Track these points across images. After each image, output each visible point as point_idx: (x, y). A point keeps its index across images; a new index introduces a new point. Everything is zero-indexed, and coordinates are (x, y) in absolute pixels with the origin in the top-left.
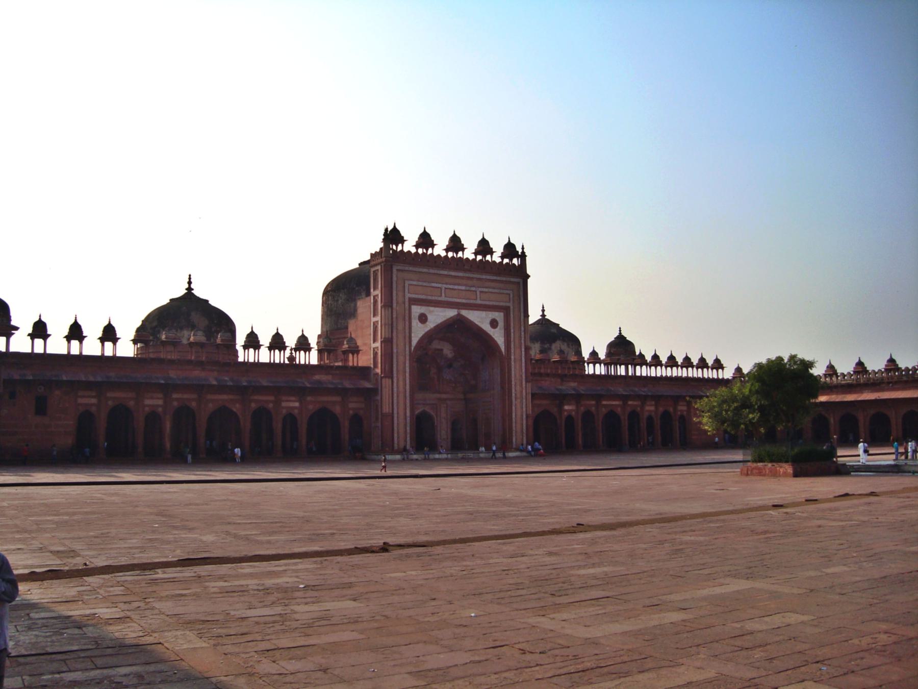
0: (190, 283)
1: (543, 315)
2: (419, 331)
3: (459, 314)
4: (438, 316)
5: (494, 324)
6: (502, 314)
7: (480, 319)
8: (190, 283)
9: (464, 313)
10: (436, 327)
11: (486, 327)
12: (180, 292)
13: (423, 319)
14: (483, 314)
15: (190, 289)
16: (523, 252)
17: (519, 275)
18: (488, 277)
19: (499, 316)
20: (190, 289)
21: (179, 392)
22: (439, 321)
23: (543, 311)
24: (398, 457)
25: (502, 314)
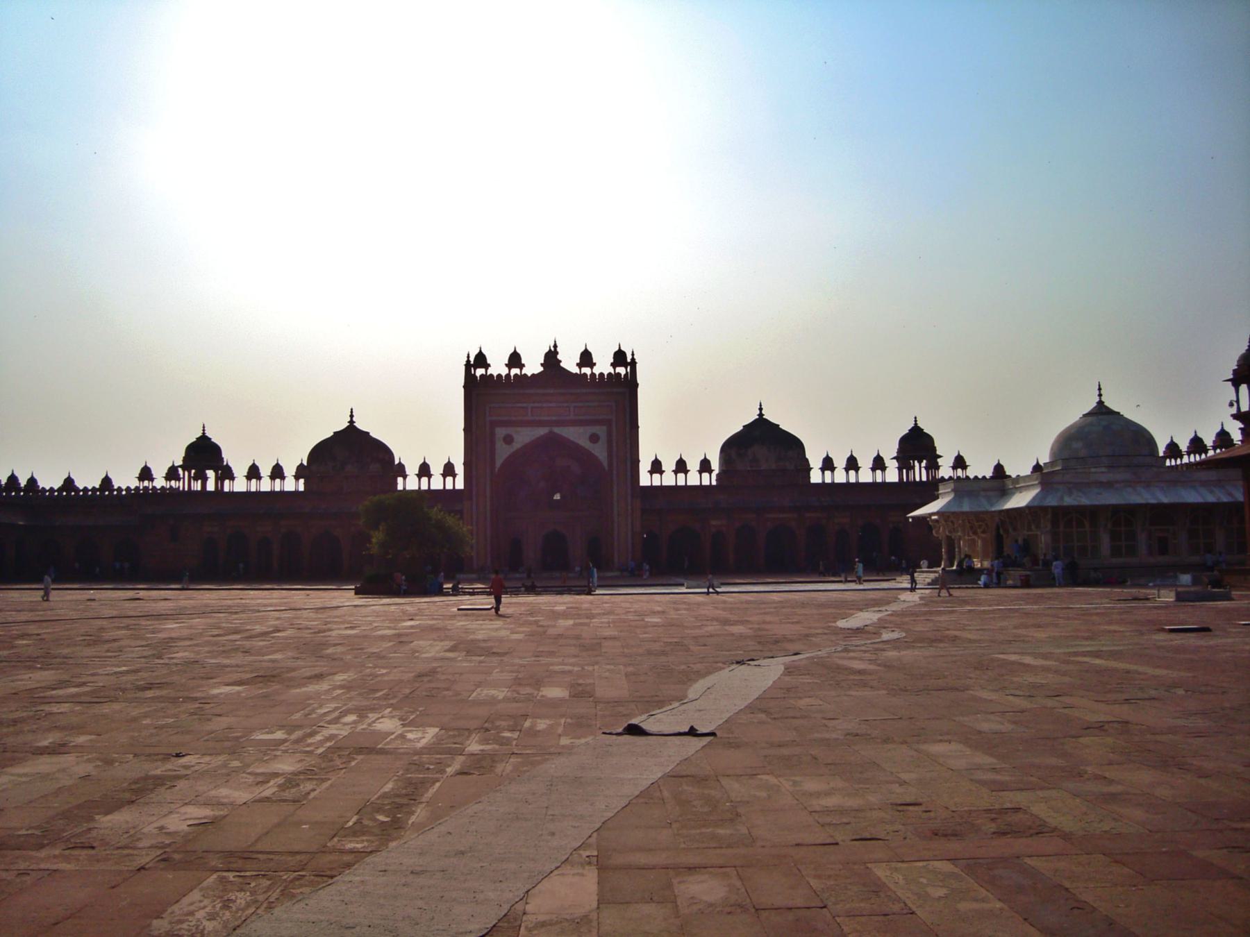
0: (352, 416)
1: (761, 415)
2: (503, 452)
3: (551, 432)
4: (524, 436)
5: (594, 438)
6: (604, 428)
7: (577, 435)
8: (352, 416)
9: (557, 430)
10: (526, 446)
11: (585, 443)
12: (343, 425)
13: (508, 440)
14: (581, 430)
15: (352, 422)
16: (633, 359)
17: (630, 384)
18: (584, 391)
19: (601, 431)
20: (352, 422)
21: (348, 515)
22: (527, 440)
23: (761, 409)
24: (474, 576)
25: (604, 428)
